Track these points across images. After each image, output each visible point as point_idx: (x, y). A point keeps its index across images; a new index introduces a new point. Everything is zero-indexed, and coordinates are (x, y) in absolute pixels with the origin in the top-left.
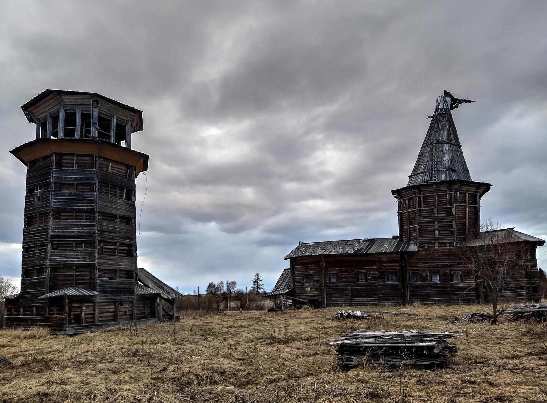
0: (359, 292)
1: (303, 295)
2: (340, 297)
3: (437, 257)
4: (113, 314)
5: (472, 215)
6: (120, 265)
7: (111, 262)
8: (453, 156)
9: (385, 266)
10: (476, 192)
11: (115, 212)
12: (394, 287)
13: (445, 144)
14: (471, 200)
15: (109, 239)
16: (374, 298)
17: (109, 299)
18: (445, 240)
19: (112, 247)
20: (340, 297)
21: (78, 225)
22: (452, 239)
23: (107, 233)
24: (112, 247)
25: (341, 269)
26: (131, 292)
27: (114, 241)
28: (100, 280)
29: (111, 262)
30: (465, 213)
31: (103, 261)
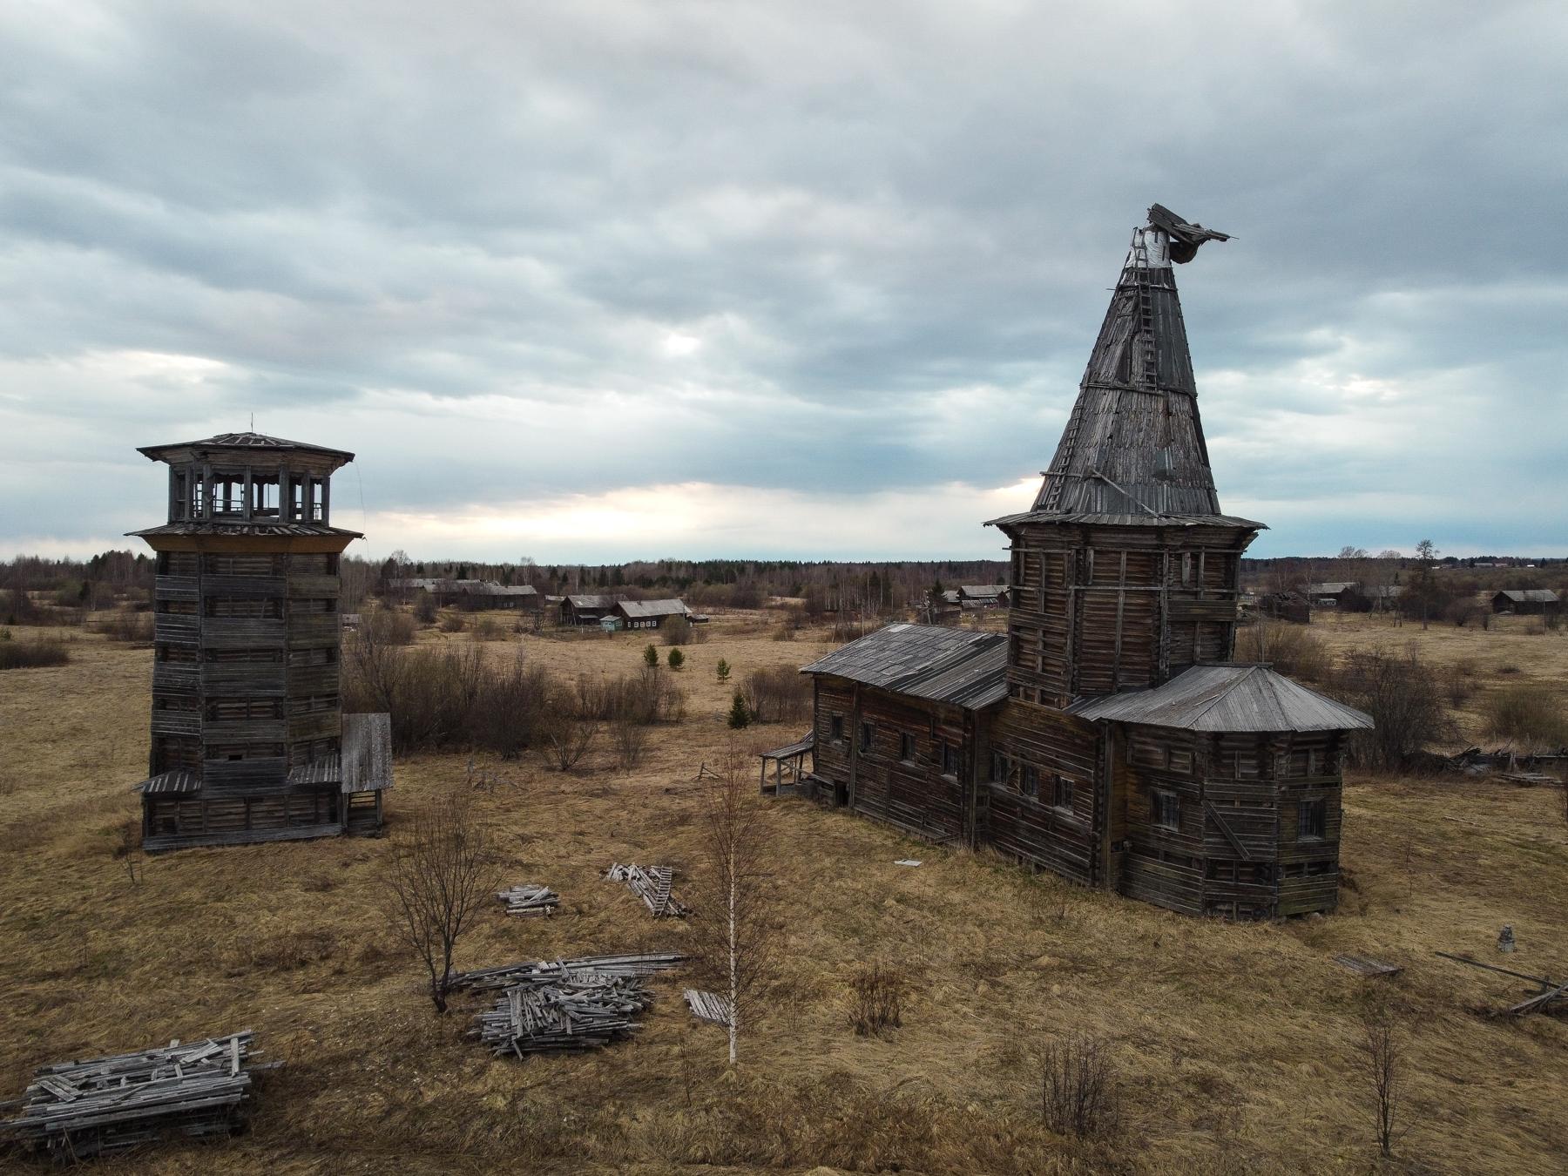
0: (901, 786)
1: (827, 767)
2: (874, 790)
3: (1035, 728)
4: (243, 816)
5: (1143, 617)
6: (255, 735)
7: (228, 732)
8: (1119, 430)
9: (944, 731)
10: (1158, 547)
11: (240, 645)
12: (951, 790)
13: (1107, 392)
14: (1143, 572)
15: (228, 692)
16: (919, 807)
17: (229, 794)
18: (1050, 685)
19: (237, 705)
20: (874, 790)
21: (180, 672)
22: (1060, 687)
23: (221, 684)
24: (237, 705)
25: (880, 720)
26: (279, 781)
27: (238, 695)
28: (208, 763)
29: (228, 732)
30: (1116, 610)
31: (214, 731)
